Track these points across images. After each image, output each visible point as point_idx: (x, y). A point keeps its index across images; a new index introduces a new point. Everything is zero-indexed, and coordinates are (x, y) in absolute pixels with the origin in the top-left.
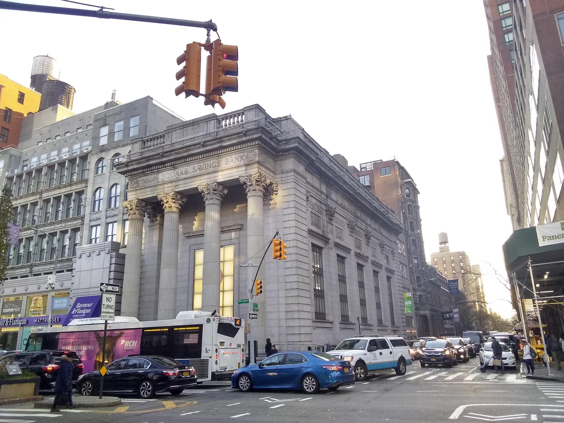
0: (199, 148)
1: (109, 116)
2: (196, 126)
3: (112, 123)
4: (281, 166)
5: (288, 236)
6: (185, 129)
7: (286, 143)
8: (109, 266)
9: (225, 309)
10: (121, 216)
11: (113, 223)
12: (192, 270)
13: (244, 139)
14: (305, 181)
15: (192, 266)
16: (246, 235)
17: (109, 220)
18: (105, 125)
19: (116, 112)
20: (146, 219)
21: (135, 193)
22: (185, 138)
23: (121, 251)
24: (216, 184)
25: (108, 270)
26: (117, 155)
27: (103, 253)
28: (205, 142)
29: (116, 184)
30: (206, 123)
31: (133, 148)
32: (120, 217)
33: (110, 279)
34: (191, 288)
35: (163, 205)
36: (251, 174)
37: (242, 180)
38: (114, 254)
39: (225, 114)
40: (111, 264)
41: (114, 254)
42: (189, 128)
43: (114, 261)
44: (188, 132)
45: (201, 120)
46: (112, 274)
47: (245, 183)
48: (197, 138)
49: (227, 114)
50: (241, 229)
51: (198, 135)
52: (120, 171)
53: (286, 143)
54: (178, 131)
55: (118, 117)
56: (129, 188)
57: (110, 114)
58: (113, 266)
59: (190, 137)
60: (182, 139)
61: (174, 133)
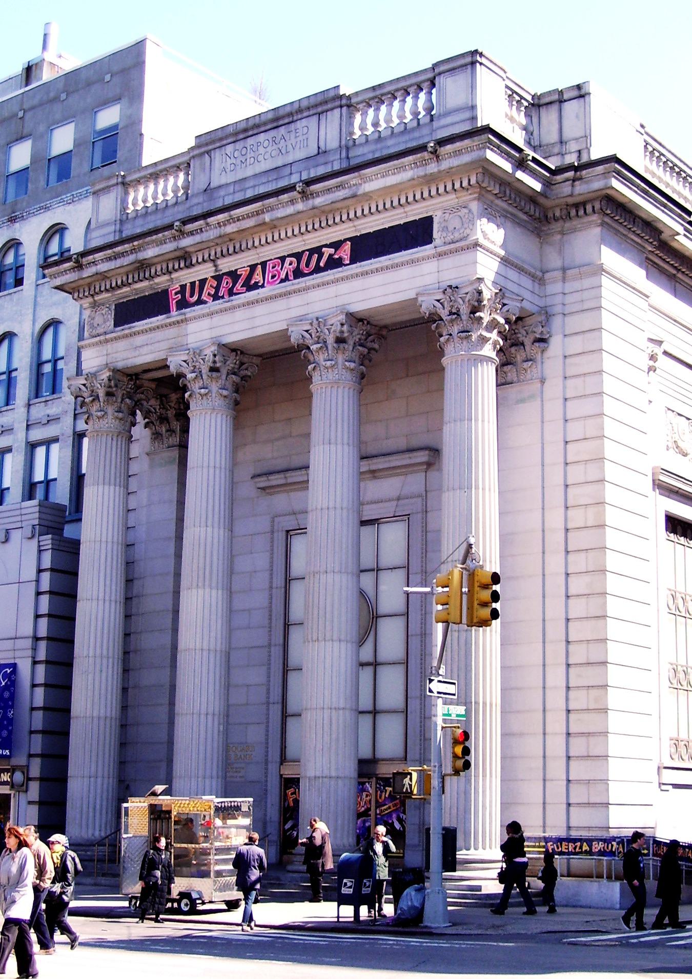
0: (292, 202)
1: (32, 108)
2: (282, 130)
3: (42, 128)
4: (560, 252)
6: (250, 141)
7: (574, 180)
8: (33, 576)
9: (381, 719)
10: (68, 420)
12: (279, 594)
14: (644, 305)
15: (279, 581)
16: (440, 489)
17: (37, 434)
18: (21, 138)
19: (52, 95)
20: (140, 432)
21: (104, 349)
22: (249, 172)
23: (69, 531)
24: (342, 317)
25: (31, 590)
26: (58, 230)
27: (16, 536)
28: (309, 183)
29: (54, 324)
30: (315, 118)
31: (96, 209)
32: (65, 427)
33: (37, 616)
34: (277, 652)
35: (185, 389)
37: (427, 304)
38: (47, 540)
39: (374, 88)
40: (40, 571)
41: (47, 540)
42: (262, 137)
43: (47, 562)
44: (261, 150)
45: (300, 111)
46: (45, 600)
47: (434, 318)
48: (287, 171)
49: (381, 86)
50: (429, 465)
51: (290, 159)
52: (58, 282)
53: (574, 180)
54: (229, 149)
55: (57, 111)
56: (86, 334)
57: (36, 101)
58: (46, 577)
61: (217, 155)
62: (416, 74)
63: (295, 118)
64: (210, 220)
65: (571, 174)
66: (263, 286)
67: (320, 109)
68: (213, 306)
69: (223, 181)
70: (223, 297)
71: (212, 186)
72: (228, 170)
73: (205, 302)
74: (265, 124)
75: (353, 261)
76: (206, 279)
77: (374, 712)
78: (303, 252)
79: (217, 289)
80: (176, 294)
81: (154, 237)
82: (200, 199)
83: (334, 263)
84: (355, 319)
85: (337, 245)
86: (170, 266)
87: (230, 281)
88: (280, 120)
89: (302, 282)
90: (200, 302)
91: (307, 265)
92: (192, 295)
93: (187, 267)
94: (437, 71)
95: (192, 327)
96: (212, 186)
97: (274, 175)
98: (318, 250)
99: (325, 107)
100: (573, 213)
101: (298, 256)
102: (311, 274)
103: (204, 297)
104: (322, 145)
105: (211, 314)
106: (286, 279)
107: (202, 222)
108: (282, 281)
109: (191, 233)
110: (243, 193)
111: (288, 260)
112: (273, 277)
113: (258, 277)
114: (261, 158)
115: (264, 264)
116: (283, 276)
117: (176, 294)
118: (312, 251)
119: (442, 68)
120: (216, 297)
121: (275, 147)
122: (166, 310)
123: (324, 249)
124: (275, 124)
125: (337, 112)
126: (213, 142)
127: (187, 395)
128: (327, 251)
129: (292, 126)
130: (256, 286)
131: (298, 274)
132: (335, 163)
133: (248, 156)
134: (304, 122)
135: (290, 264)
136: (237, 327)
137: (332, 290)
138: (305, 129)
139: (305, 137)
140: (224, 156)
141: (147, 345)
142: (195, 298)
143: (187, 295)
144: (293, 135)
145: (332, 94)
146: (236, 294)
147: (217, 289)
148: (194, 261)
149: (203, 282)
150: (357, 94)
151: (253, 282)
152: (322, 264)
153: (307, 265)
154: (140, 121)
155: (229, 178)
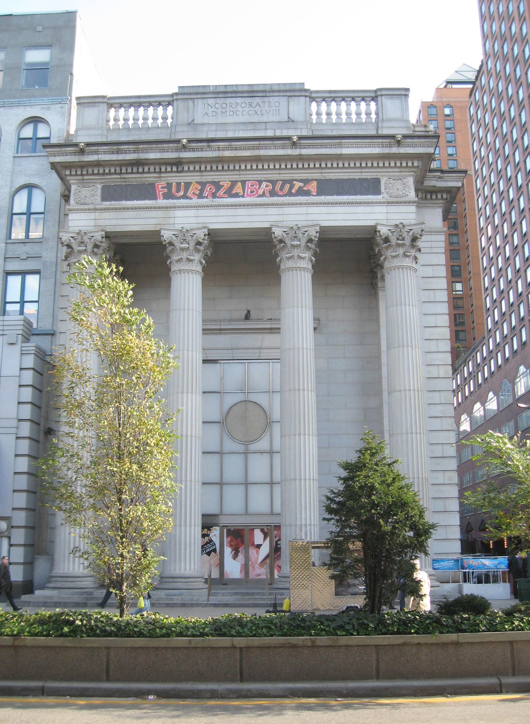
0: (283, 147)
2: (257, 100)
5: (434, 356)
6: (229, 100)
7: (440, 177)
11: (23, 273)
13: (395, 150)
21: (92, 215)
22: (229, 120)
30: (286, 99)
36: (405, 222)
42: (239, 100)
44: (239, 108)
51: (265, 119)
53: (440, 177)
54: (211, 101)
59: (241, 119)
60: (221, 120)
62: (354, 91)
63: (268, 95)
64: (211, 144)
65: (439, 174)
66: (243, 196)
67: (289, 94)
68: (195, 201)
69: (206, 120)
70: (207, 197)
71: (195, 122)
72: (210, 115)
73: (190, 198)
74: (242, 92)
75: (319, 194)
76: (191, 183)
77: (272, 483)
78: (278, 180)
79: (202, 191)
80: (162, 188)
81: (159, 146)
82: (186, 128)
83: (301, 192)
84: (211, 233)
85: (306, 182)
86: (163, 169)
87: (213, 187)
88: (253, 92)
89: (275, 199)
90: (185, 197)
91: (282, 189)
92: (178, 191)
93: (178, 172)
94: (379, 93)
95: (179, 213)
96: (195, 122)
97: (251, 127)
98: (290, 182)
99: (292, 94)
100: (429, 196)
101: (274, 183)
102: (285, 195)
103: (189, 194)
104: (291, 116)
105: (197, 207)
106: (263, 195)
107: (205, 144)
108: (260, 196)
109: (193, 150)
110: (224, 133)
111: (264, 184)
112: (251, 192)
113: (238, 188)
114: (238, 113)
115: (243, 183)
116: (261, 192)
117: (162, 188)
118: (285, 182)
119: (384, 93)
120: (200, 196)
121: (251, 109)
122: (154, 197)
123: (294, 182)
124: (251, 95)
125: (303, 99)
126: (197, 93)
127: (382, 258)
128: (298, 185)
129: (266, 99)
130: (237, 195)
131: (273, 193)
132: (303, 130)
133: (228, 110)
134: (276, 99)
135: (267, 186)
136: (221, 220)
137: (303, 210)
138: (277, 104)
139: (277, 108)
140: (206, 106)
141: (134, 218)
142: (181, 193)
143: (174, 190)
144: (267, 104)
145: (298, 87)
146: (219, 197)
147: (202, 191)
148: (186, 168)
149: (188, 185)
150: (317, 92)
151: (234, 192)
152: (293, 191)
153: (282, 189)
154: (71, 65)
155: (212, 120)
